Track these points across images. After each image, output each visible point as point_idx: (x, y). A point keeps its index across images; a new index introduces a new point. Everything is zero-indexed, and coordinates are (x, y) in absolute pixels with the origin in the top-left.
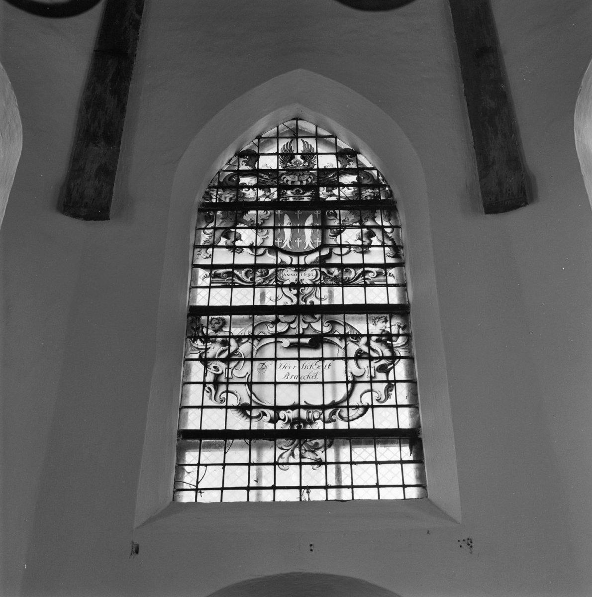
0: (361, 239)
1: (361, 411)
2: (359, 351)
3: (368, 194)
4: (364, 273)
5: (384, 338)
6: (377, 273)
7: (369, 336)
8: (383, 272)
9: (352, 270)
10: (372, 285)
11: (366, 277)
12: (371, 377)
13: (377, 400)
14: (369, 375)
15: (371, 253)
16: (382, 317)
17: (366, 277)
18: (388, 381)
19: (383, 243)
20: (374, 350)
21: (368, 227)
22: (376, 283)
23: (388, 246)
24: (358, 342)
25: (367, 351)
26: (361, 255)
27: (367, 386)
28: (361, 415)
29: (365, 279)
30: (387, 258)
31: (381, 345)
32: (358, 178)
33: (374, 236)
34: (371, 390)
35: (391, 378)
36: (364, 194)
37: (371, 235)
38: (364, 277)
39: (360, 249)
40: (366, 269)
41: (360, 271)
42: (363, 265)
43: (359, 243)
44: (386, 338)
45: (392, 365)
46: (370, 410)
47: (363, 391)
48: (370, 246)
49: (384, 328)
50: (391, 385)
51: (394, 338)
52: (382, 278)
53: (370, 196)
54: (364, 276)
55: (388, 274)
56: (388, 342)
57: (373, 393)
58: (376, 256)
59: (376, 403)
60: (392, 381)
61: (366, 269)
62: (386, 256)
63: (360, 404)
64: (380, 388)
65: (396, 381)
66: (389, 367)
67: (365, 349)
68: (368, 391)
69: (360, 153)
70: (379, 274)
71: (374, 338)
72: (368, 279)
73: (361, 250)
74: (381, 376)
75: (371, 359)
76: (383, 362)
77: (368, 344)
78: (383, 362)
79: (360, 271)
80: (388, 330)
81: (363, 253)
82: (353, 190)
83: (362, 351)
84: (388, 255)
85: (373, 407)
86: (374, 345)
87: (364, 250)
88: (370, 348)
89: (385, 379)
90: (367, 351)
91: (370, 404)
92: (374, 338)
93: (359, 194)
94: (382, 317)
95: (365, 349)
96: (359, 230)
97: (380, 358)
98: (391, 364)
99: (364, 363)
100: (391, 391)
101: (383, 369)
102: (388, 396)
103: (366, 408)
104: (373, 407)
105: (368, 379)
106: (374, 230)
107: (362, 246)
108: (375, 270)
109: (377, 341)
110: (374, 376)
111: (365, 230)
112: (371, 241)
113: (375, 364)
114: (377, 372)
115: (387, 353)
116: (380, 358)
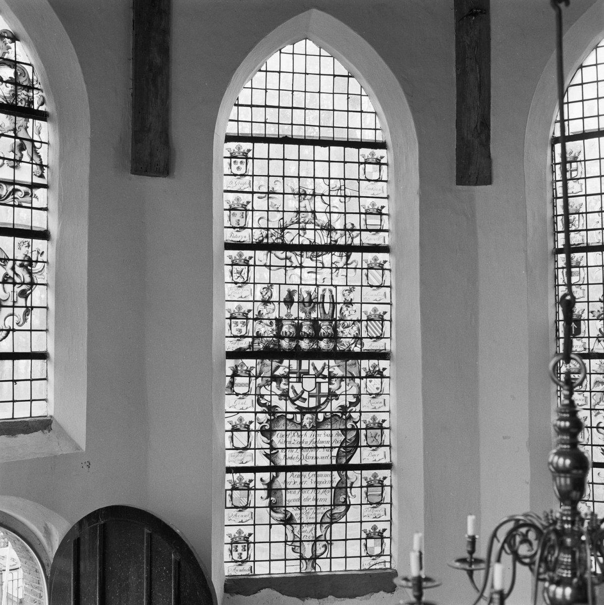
0: (14, 151)
1: (4, 333)
2: (6, 275)
3: (23, 96)
4: (14, 191)
5: (26, 263)
6: (25, 193)
7: (14, 260)
8: (30, 192)
9: (4, 186)
10: (20, 206)
11: (16, 196)
12: (14, 302)
13: (17, 324)
14: (12, 300)
15: (21, 169)
16: (26, 242)
17: (16, 196)
18: (26, 307)
19: (32, 159)
20: (17, 275)
21: (21, 139)
22: (24, 204)
23: (36, 164)
24: (5, 265)
25: (12, 276)
26: (12, 169)
27: (10, 310)
28: (4, 338)
29: (14, 198)
30: (34, 176)
31: (23, 270)
32: (16, 73)
33: (25, 150)
34: (13, 315)
35: (29, 305)
36: (19, 96)
37: (22, 148)
38: (14, 196)
39: (12, 163)
40: (17, 187)
41: (11, 188)
42: (13, 183)
43: (12, 156)
44: (28, 263)
45: (30, 291)
46: (11, 332)
47: (6, 315)
48: (20, 161)
49: (26, 253)
50: (29, 309)
51: (34, 263)
52: (28, 199)
53: (24, 99)
54: (14, 194)
55: (34, 195)
56: (29, 268)
57: (15, 316)
58: (25, 174)
59: (16, 327)
60: (29, 307)
61: (17, 187)
62: (33, 174)
63: (4, 328)
64: (20, 312)
65: (32, 308)
66: (28, 292)
67: (11, 273)
68: (11, 315)
69: (19, 40)
70: (26, 194)
71: (18, 263)
72: (17, 198)
73: (13, 164)
74: (21, 302)
75: (14, 283)
76: (24, 287)
77: (13, 269)
78: (24, 287)
79: (11, 188)
80: (29, 255)
81: (14, 167)
82: (10, 88)
83: (8, 275)
84: (35, 173)
85: (14, 330)
86: (19, 270)
87: (16, 164)
88: (15, 273)
89: (24, 305)
90: (12, 276)
91: (12, 328)
92: (18, 263)
93: (15, 95)
94: (26, 242)
95: (11, 273)
96: (13, 140)
97: (22, 284)
98: (29, 290)
99: (9, 287)
100: (28, 315)
101: (23, 294)
102: (25, 320)
103: (8, 331)
104: (14, 330)
105: (11, 304)
106: (26, 142)
107: (14, 160)
108: (23, 189)
109: (21, 266)
110: (15, 300)
111: (18, 140)
112: (22, 155)
113: (18, 289)
114: (18, 298)
115: (28, 280)
116: (22, 284)
